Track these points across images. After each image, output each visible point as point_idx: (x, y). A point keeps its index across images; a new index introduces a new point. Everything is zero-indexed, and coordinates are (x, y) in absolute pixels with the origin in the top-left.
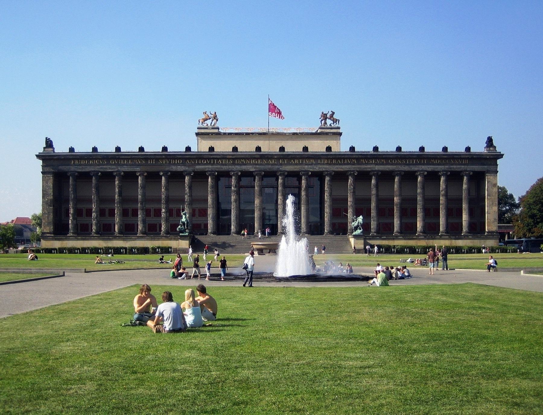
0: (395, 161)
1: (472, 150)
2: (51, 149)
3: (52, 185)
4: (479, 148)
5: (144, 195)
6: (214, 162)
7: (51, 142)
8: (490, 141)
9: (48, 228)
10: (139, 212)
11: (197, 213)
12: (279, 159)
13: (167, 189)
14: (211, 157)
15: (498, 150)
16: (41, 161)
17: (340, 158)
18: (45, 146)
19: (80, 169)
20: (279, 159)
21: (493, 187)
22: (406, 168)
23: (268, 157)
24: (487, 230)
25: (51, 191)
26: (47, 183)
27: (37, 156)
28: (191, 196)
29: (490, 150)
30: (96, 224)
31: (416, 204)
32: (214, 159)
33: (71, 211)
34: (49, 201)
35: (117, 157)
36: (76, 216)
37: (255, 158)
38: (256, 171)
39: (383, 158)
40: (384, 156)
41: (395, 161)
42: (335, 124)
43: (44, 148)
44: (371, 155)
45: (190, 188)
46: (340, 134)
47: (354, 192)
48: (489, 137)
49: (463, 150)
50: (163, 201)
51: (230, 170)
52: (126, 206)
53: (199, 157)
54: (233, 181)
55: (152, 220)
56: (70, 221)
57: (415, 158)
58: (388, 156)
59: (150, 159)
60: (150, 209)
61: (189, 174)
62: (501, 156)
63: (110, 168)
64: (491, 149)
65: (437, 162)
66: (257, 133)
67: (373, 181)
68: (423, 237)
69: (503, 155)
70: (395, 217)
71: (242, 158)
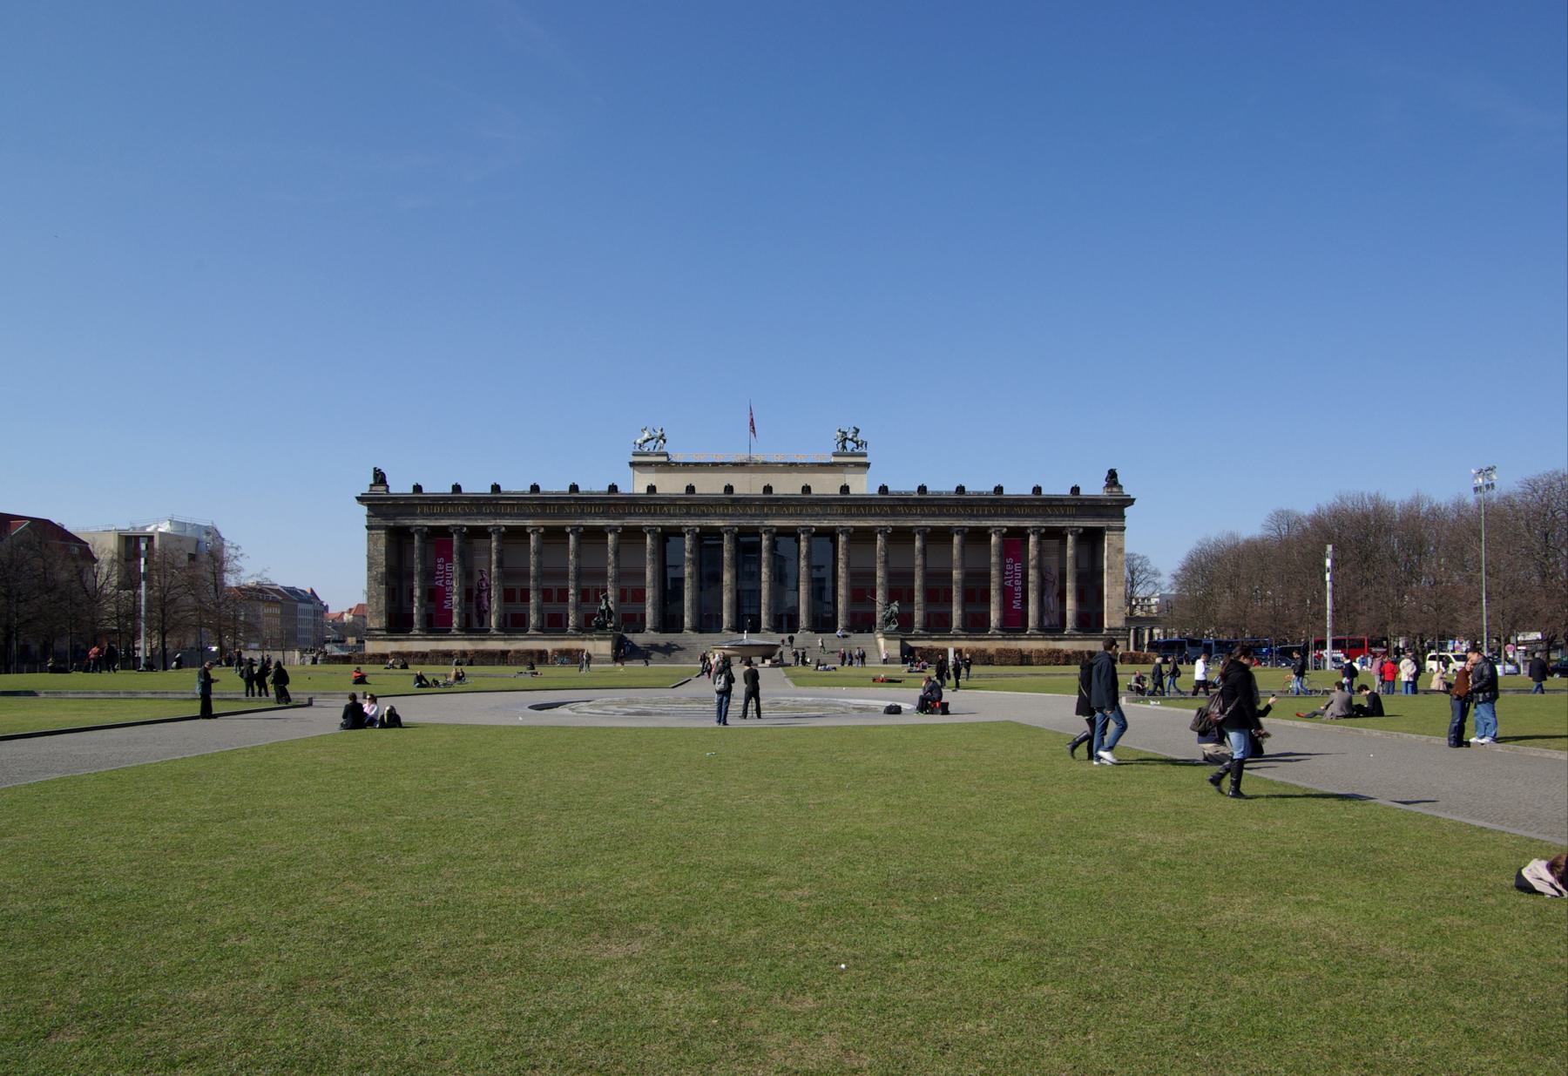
0: (954, 511)
1: (1083, 492)
2: (384, 488)
3: (384, 548)
4: (1094, 487)
5: (539, 564)
6: (655, 510)
7: (383, 474)
8: (1112, 475)
9: (377, 621)
10: (532, 594)
11: (629, 594)
13: (578, 556)
15: (1126, 491)
16: (366, 508)
17: (863, 505)
18: (372, 482)
21: (1118, 555)
22: (973, 523)
23: (745, 503)
24: (1106, 626)
25: (382, 559)
26: (375, 544)
27: (357, 498)
28: (617, 567)
29: (1111, 492)
30: (460, 615)
31: (989, 581)
32: (655, 505)
33: (417, 592)
34: (379, 576)
35: (495, 502)
36: (425, 602)
37: (723, 505)
38: (725, 526)
39: (934, 506)
40: (936, 503)
41: (954, 511)
42: (860, 448)
43: (371, 485)
45: (617, 553)
46: (867, 465)
47: (886, 562)
48: (1112, 470)
49: (1066, 492)
50: (571, 576)
52: (511, 584)
53: (633, 504)
54: (687, 542)
55: (554, 607)
56: (415, 609)
57: (987, 506)
58: (942, 502)
59: (550, 505)
60: (551, 590)
61: (614, 529)
62: (1131, 501)
64: (1115, 489)
65: (1024, 511)
66: (731, 463)
67: (918, 544)
68: (1000, 637)
69: (1134, 500)
70: (954, 603)
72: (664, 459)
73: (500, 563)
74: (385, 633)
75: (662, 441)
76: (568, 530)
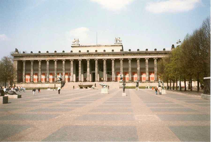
2: (17, 52)
7: (17, 50)
12: (95, 55)
14: (71, 54)
19: (26, 59)
20: (95, 55)
32: (72, 55)
40: (133, 53)
43: (15, 52)
44: (128, 52)
51: (78, 59)
63: (37, 59)
71: (83, 55)
72: (78, 45)
73: (41, 68)
74: (17, 83)
75: (78, 42)
76: (54, 60)
